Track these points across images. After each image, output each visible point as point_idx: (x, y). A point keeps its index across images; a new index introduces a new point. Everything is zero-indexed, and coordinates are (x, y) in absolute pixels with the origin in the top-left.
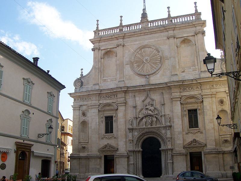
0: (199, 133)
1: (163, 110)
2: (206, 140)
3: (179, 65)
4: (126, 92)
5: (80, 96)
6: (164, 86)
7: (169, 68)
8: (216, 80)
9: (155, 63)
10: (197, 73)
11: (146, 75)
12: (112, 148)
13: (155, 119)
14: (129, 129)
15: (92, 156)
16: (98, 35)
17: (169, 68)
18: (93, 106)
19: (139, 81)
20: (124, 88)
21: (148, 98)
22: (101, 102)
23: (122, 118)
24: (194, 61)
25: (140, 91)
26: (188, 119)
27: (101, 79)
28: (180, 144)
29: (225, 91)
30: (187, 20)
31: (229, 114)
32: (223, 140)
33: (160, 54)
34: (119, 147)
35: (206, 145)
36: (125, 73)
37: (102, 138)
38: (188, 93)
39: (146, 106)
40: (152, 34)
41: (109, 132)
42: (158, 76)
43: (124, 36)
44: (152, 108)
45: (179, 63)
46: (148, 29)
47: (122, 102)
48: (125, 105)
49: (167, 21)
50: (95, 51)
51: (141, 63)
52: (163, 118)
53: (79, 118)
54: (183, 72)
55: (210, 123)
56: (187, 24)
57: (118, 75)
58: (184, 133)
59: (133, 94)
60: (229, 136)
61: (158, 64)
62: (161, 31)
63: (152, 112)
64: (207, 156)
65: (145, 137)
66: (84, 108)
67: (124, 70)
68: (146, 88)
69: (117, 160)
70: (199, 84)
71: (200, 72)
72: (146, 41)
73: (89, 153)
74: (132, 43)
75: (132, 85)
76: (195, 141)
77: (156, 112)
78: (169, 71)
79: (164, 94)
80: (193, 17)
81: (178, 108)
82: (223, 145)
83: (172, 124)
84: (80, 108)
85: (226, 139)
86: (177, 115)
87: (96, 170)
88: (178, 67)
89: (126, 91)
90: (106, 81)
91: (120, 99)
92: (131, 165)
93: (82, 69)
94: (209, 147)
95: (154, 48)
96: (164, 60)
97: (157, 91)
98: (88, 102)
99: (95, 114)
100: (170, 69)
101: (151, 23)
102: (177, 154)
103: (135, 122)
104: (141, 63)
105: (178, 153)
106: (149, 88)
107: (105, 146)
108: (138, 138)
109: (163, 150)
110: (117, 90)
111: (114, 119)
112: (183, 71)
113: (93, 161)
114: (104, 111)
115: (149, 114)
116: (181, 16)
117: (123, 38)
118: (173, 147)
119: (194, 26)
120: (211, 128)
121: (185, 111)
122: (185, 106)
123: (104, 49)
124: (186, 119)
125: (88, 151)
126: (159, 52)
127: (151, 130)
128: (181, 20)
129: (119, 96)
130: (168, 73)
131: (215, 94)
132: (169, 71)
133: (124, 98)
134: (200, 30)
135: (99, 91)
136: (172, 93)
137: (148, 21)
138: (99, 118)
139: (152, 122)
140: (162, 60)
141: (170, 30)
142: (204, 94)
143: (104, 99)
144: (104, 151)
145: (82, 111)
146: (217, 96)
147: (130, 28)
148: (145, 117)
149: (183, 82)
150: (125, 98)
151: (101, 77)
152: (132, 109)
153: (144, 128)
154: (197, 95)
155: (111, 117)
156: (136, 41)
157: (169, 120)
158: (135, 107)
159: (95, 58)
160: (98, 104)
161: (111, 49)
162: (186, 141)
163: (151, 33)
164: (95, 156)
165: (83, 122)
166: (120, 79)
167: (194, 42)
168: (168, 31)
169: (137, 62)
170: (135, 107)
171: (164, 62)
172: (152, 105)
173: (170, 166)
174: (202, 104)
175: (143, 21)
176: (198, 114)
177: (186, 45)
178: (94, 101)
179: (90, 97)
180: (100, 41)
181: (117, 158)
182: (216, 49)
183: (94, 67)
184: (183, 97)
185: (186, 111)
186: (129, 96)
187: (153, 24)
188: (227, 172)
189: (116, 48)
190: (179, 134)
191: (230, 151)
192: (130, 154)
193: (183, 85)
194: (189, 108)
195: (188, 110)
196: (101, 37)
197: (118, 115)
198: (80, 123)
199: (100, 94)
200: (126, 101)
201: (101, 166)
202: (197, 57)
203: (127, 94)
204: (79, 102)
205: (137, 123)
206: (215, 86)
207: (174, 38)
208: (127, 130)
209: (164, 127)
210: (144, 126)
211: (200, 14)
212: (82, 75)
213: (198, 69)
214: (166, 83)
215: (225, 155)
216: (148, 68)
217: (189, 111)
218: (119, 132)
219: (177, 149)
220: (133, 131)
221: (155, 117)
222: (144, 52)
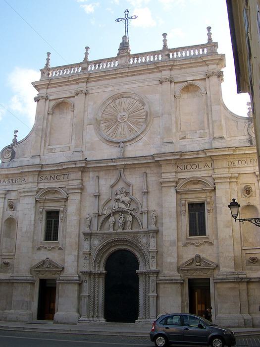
0: (206, 245)
1: (145, 204)
2: (218, 257)
3: (177, 127)
4: (83, 170)
5: (7, 174)
6: (149, 161)
7: (159, 131)
8: (238, 153)
9: (137, 123)
10: (206, 141)
11: (119, 143)
13: (130, 218)
14: (85, 234)
15: (18, 280)
16: (47, 76)
17: (160, 132)
18: (27, 192)
19: (107, 152)
22: (41, 186)
24: (203, 122)
25: (107, 169)
26: (188, 219)
27: (44, 148)
28: (171, 263)
29: (254, 173)
30: (194, 54)
32: (248, 258)
33: (146, 108)
34: (66, 265)
37: (39, 249)
38: (189, 173)
39: (117, 194)
40: (134, 75)
42: (140, 144)
43: (88, 78)
44: (127, 199)
45: (176, 123)
46: (129, 67)
47: (77, 187)
48: (81, 193)
49: (160, 56)
50: (40, 101)
51: (113, 121)
54: (183, 139)
55: (227, 227)
56: (192, 60)
57: (73, 142)
58: (180, 244)
59: (96, 174)
61: (142, 124)
62: (150, 71)
64: (219, 286)
65: (113, 249)
66: (13, 195)
67: (84, 134)
68: (119, 164)
70: (209, 159)
72: (124, 87)
73: (15, 274)
74: (101, 90)
76: (198, 258)
77: (133, 206)
78: (159, 137)
79: (148, 175)
80: (203, 51)
81: (170, 200)
82: (249, 267)
83: (159, 228)
85: (253, 256)
86: (169, 212)
88: (174, 130)
89: (84, 167)
91: (74, 180)
92: (85, 297)
93: (16, 132)
94: (222, 269)
95: (137, 98)
100: (161, 133)
101: (134, 58)
103: (95, 222)
104: (113, 121)
105: (167, 280)
107: (41, 262)
108: (100, 251)
109: (142, 273)
110: (68, 166)
111: (61, 215)
112: (183, 136)
114: (45, 201)
115: (121, 210)
116: (185, 48)
118: (159, 268)
119: (205, 63)
120: (227, 237)
121: (184, 205)
122: (183, 196)
124: (185, 220)
125: (13, 270)
126: (144, 104)
127: (122, 237)
128: (184, 55)
129: (72, 176)
131: (237, 178)
132: (159, 137)
133: (80, 181)
135: (38, 167)
137: (129, 55)
138: (35, 213)
139: (125, 223)
140: (148, 117)
141: (164, 70)
142: (217, 176)
143: (46, 181)
144: (39, 271)
147: (99, 66)
148: (114, 213)
149: (181, 155)
150: (82, 180)
151: (45, 146)
152: (93, 199)
153: (111, 234)
155: (57, 212)
156: (107, 86)
157: (155, 220)
159: (38, 113)
160: (36, 189)
161: (65, 99)
162: (182, 258)
163: (133, 74)
164: (23, 280)
165: (9, 218)
166: (75, 148)
167: (203, 90)
168: (161, 71)
170: (98, 196)
171: (152, 121)
172: (127, 194)
173: (152, 302)
174: (213, 194)
175: (121, 55)
176: (206, 210)
177: (190, 95)
178: (31, 184)
179: (25, 177)
180: (48, 86)
182: (238, 92)
183: (35, 129)
184: (181, 181)
186: (89, 177)
187: (138, 60)
188: (254, 316)
190: (170, 246)
192: (83, 278)
193: (181, 160)
194: (191, 201)
195: (189, 204)
196: (50, 79)
198: (4, 221)
199: (40, 172)
200: (82, 185)
201: (33, 298)
202: (208, 114)
203: (85, 174)
205: (100, 224)
206: (236, 163)
207: (171, 82)
208: (82, 235)
210: (111, 230)
211: (216, 45)
212: (15, 141)
214: (152, 156)
215: (252, 286)
216: (123, 132)
217: (191, 206)
218: (68, 239)
219: (166, 272)
220: (91, 238)
221: (131, 214)
222: (119, 104)
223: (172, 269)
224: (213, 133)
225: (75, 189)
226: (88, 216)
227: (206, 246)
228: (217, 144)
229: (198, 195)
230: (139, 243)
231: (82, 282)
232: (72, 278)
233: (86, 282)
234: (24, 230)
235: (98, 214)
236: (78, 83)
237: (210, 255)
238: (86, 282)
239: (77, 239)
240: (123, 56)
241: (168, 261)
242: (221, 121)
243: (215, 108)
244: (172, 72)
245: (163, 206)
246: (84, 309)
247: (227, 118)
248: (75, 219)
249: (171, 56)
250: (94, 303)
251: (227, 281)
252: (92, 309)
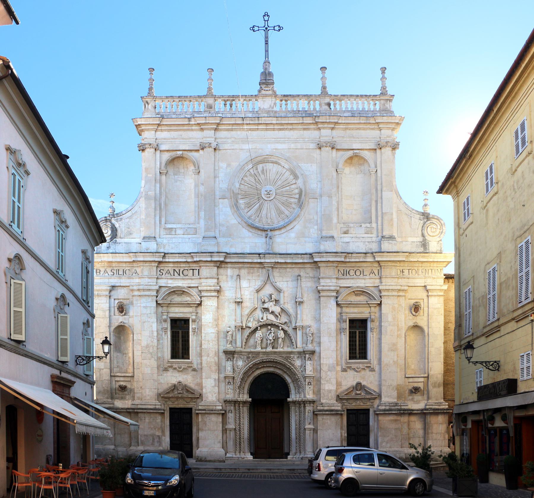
2: (380, 386)
3: (338, 215)
4: (220, 264)
5: (111, 262)
7: (316, 218)
9: (287, 205)
11: (267, 231)
12: (188, 391)
13: (281, 334)
14: (226, 352)
15: (145, 409)
20: (220, 256)
21: (269, 282)
22: (162, 282)
23: (210, 325)
24: (370, 212)
27: (160, 227)
28: (330, 391)
29: (425, 286)
31: (426, 334)
32: (410, 388)
33: (300, 182)
34: (204, 390)
35: (380, 396)
36: (217, 220)
37: (166, 370)
38: (352, 281)
39: (264, 302)
41: (181, 355)
43: (218, 124)
44: (277, 310)
47: (213, 288)
48: (218, 297)
52: (299, 333)
53: (110, 316)
54: (346, 233)
55: (392, 350)
59: (236, 272)
60: (422, 380)
63: (276, 316)
64: (381, 418)
66: (121, 294)
67: (217, 212)
69: (200, 420)
70: (376, 265)
71: (380, 238)
73: (137, 402)
74: (236, 146)
75: (233, 250)
82: (411, 397)
84: (113, 293)
85: (416, 385)
86: (328, 329)
87: (153, 439)
88: (335, 220)
89: (222, 262)
90: (173, 233)
92: (231, 430)
94: (384, 399)
95: (287, 166)
96: (307, 199)
97: (288, 270)
98: (132, 280)
99: (149, 312)
102: (324, 413)
106: (273, 261)
107: (172, 386)
108: (245, 373)
109: (294, 402)
111: (192, 326)
112: (345, 229)
113: (147, 420)
114: (169, 305)
115: (270, 323)
117: (216, 130)
120: (391, 362)
122: (345, 310)
123: (168, 151)
126: (296, 177)
127: (272, 357)
130: (314, 232)
132: (316, 227)
134: (388, 139)
136: (319, 279)
139: (276, 339)
143: (168, 276)
144: (169, 398)
145: (117, 301)
146: (409, 295)
149: (345, 257)
150: (218, 279)
152: (233, 306)
153: (258, 353)
154: (370, 288)
155: (186, 321)
157: (311, 339)
158: (239, 303)
160: (157, 287)
161: (184, 152)
166: (205, 232)
167: (372, 165)
168: (319, 129)
169: (245, 196)
170: (239, 303)
177: (353, 169)
181: (200, 416)
185: (346, 322)
189: (197, 151)
190: (329, 370)
191: (422, 410)
192: (228, 408)
195: (350, 320)
197: (203, 317)
198: (112, 328)
201: (163, 432)
202: (376, 202)
204: (109, 278)
205: (244, 341)
206: (406, 272)
209: (299, 353)
210: (259, 349)
213: (377, 230)
214: (310, 254)
217: (352, 322)
218: (204, 358)
219: (323, 401)
220: (233, 358)
221: (282, 329)
223: (330, 398)
224: (382, 230)
225: (210, 291)
226: (228, 329)
227: (367, 372)
228: (386, 246)
229: (361, 309)
231: (226, 411)
232: (214, 408)
233: (231, 412)
234: (144, 343)
235: (242, 326)
236: (202, 130)
237: (370, 383)
238: (231, 412)
239: (216, 358)
240: (266, 96)
241: (327, 388)
242: (392, 214)
243: (386, 194)
244: (334, 131)
245: (322, 321)
246: (231, 444)
247: (399, 211)
248: (213, 331)
249: (332, 107)
250: (240, 437)
251: (390, 412)
252: (238, 445)
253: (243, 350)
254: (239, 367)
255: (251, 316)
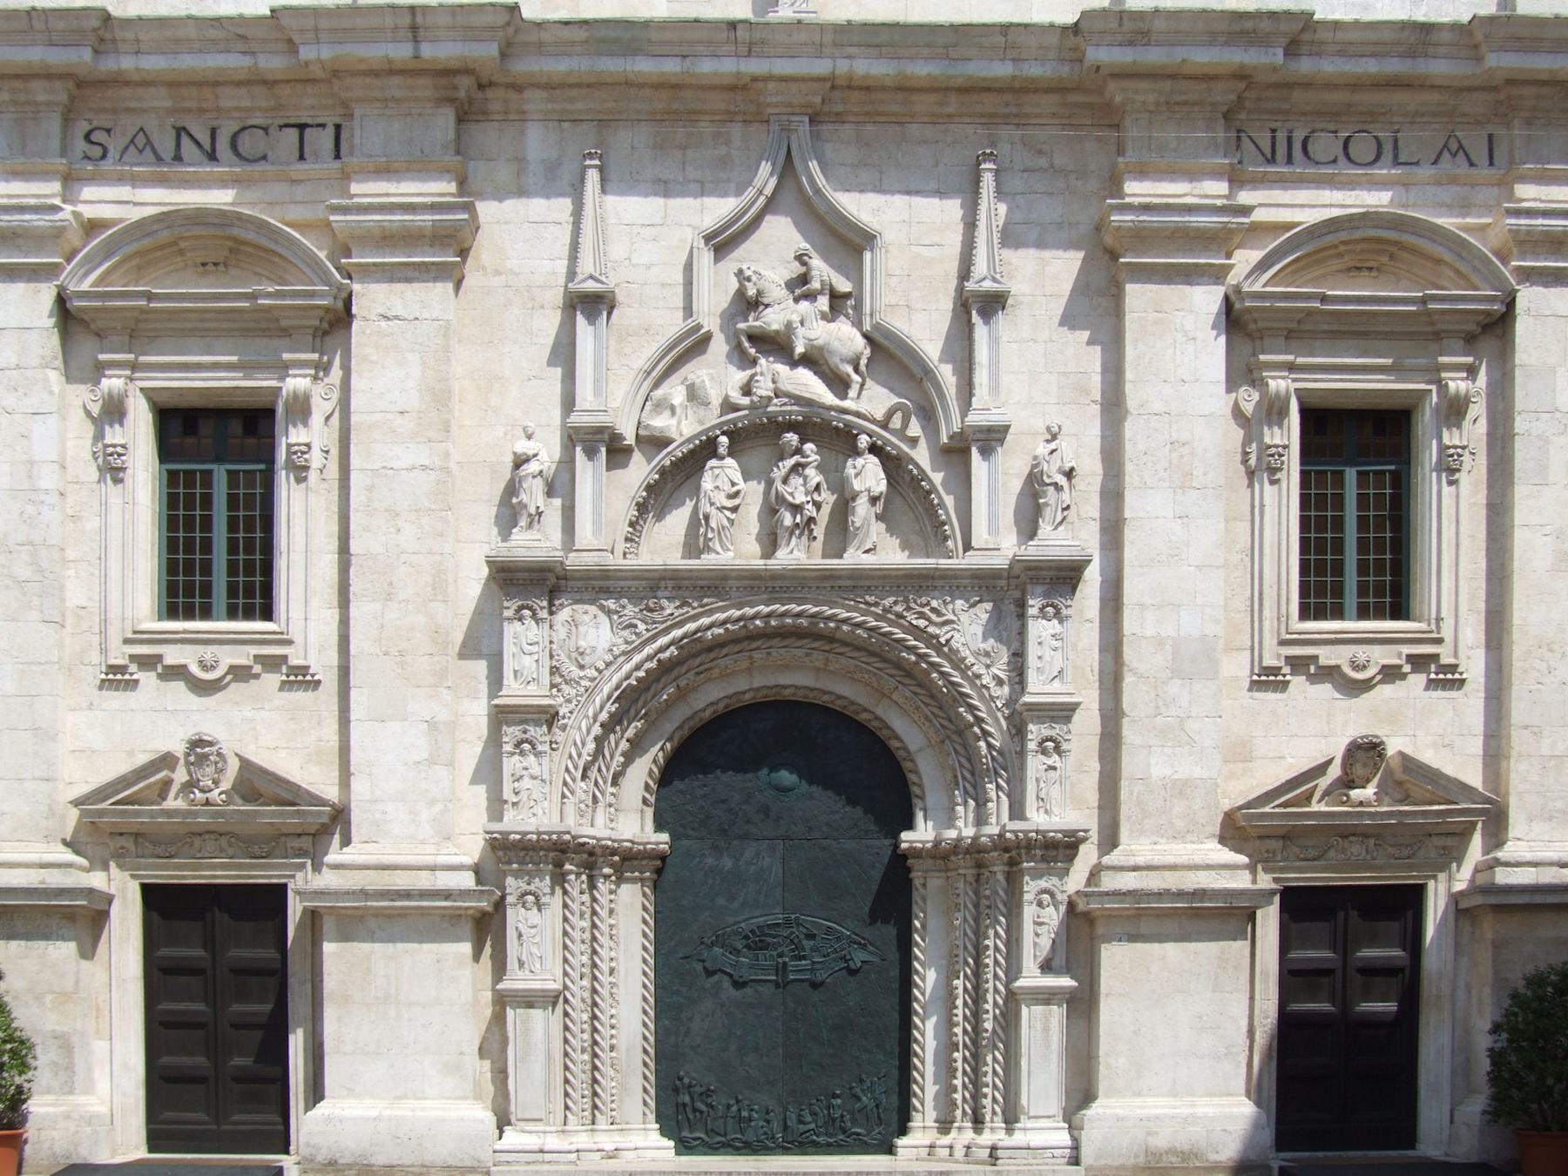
0: (1418, 680)
13: (868, 475)
44: (844, 338)
63: (839, 384)
115: (795, 412)
153: (716, 585)
190: (1176, 673)
230: (938, 648)
253: (615, 561)
254: (587, 660)
255: (675, 378)
